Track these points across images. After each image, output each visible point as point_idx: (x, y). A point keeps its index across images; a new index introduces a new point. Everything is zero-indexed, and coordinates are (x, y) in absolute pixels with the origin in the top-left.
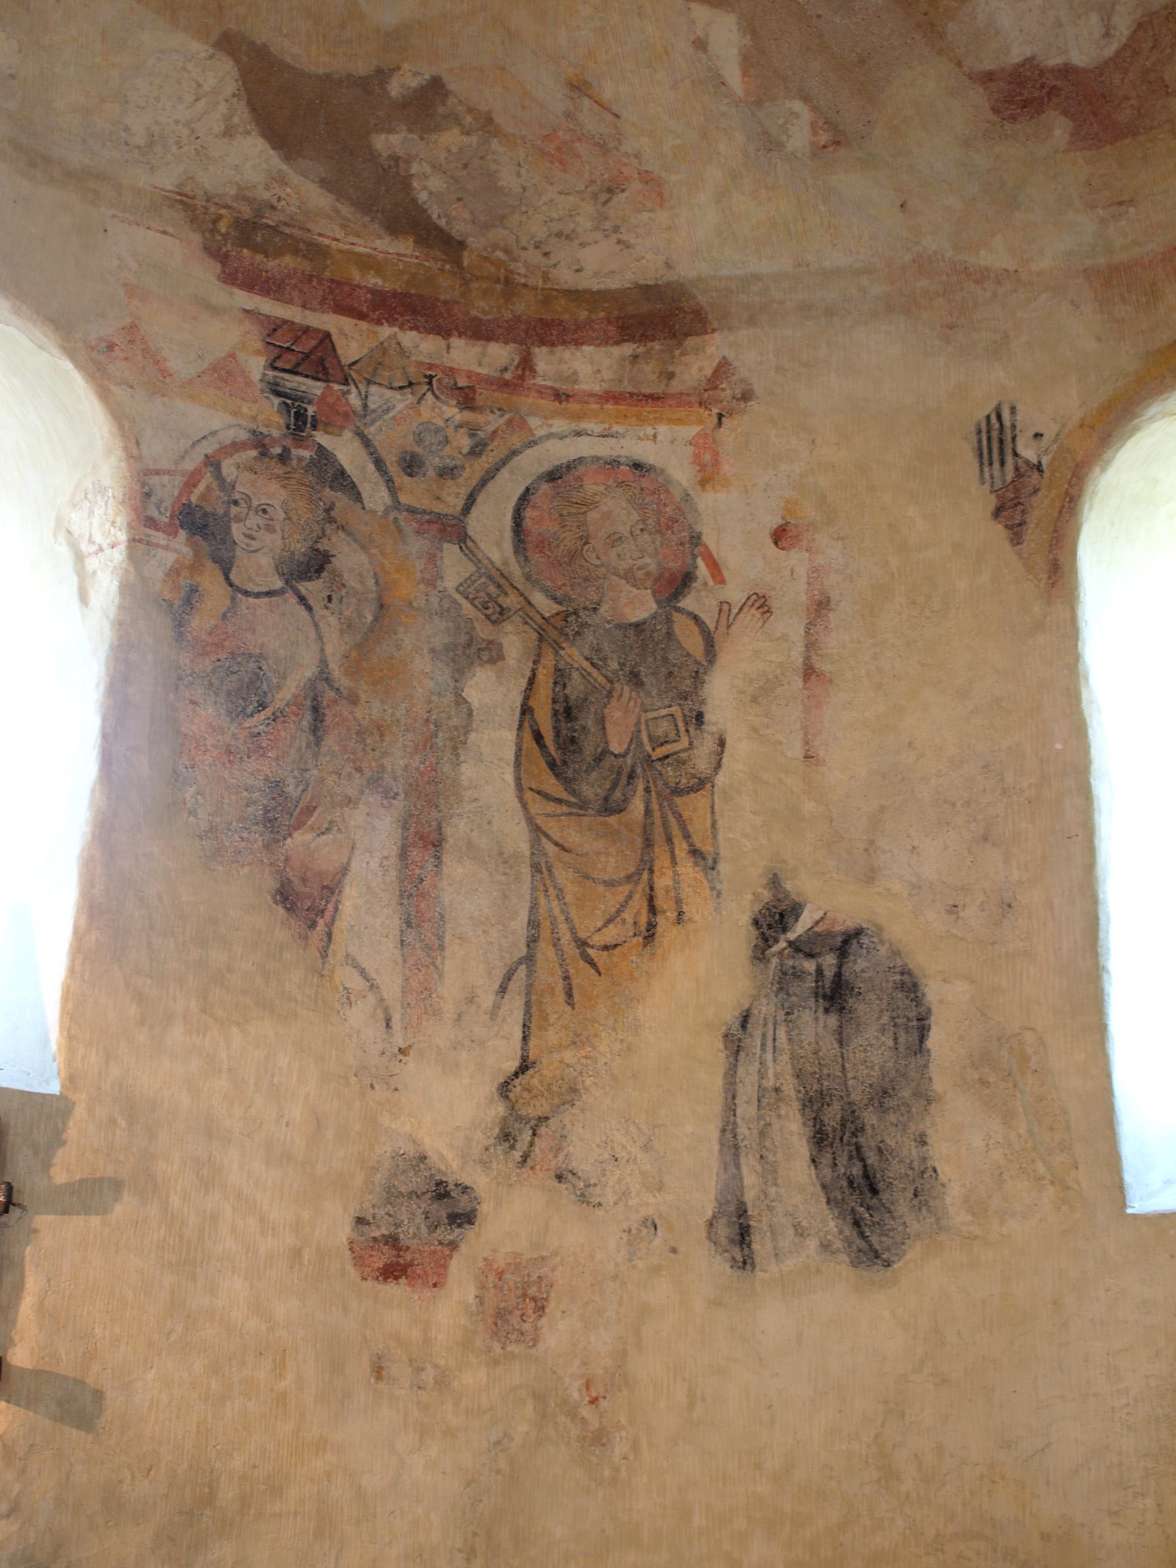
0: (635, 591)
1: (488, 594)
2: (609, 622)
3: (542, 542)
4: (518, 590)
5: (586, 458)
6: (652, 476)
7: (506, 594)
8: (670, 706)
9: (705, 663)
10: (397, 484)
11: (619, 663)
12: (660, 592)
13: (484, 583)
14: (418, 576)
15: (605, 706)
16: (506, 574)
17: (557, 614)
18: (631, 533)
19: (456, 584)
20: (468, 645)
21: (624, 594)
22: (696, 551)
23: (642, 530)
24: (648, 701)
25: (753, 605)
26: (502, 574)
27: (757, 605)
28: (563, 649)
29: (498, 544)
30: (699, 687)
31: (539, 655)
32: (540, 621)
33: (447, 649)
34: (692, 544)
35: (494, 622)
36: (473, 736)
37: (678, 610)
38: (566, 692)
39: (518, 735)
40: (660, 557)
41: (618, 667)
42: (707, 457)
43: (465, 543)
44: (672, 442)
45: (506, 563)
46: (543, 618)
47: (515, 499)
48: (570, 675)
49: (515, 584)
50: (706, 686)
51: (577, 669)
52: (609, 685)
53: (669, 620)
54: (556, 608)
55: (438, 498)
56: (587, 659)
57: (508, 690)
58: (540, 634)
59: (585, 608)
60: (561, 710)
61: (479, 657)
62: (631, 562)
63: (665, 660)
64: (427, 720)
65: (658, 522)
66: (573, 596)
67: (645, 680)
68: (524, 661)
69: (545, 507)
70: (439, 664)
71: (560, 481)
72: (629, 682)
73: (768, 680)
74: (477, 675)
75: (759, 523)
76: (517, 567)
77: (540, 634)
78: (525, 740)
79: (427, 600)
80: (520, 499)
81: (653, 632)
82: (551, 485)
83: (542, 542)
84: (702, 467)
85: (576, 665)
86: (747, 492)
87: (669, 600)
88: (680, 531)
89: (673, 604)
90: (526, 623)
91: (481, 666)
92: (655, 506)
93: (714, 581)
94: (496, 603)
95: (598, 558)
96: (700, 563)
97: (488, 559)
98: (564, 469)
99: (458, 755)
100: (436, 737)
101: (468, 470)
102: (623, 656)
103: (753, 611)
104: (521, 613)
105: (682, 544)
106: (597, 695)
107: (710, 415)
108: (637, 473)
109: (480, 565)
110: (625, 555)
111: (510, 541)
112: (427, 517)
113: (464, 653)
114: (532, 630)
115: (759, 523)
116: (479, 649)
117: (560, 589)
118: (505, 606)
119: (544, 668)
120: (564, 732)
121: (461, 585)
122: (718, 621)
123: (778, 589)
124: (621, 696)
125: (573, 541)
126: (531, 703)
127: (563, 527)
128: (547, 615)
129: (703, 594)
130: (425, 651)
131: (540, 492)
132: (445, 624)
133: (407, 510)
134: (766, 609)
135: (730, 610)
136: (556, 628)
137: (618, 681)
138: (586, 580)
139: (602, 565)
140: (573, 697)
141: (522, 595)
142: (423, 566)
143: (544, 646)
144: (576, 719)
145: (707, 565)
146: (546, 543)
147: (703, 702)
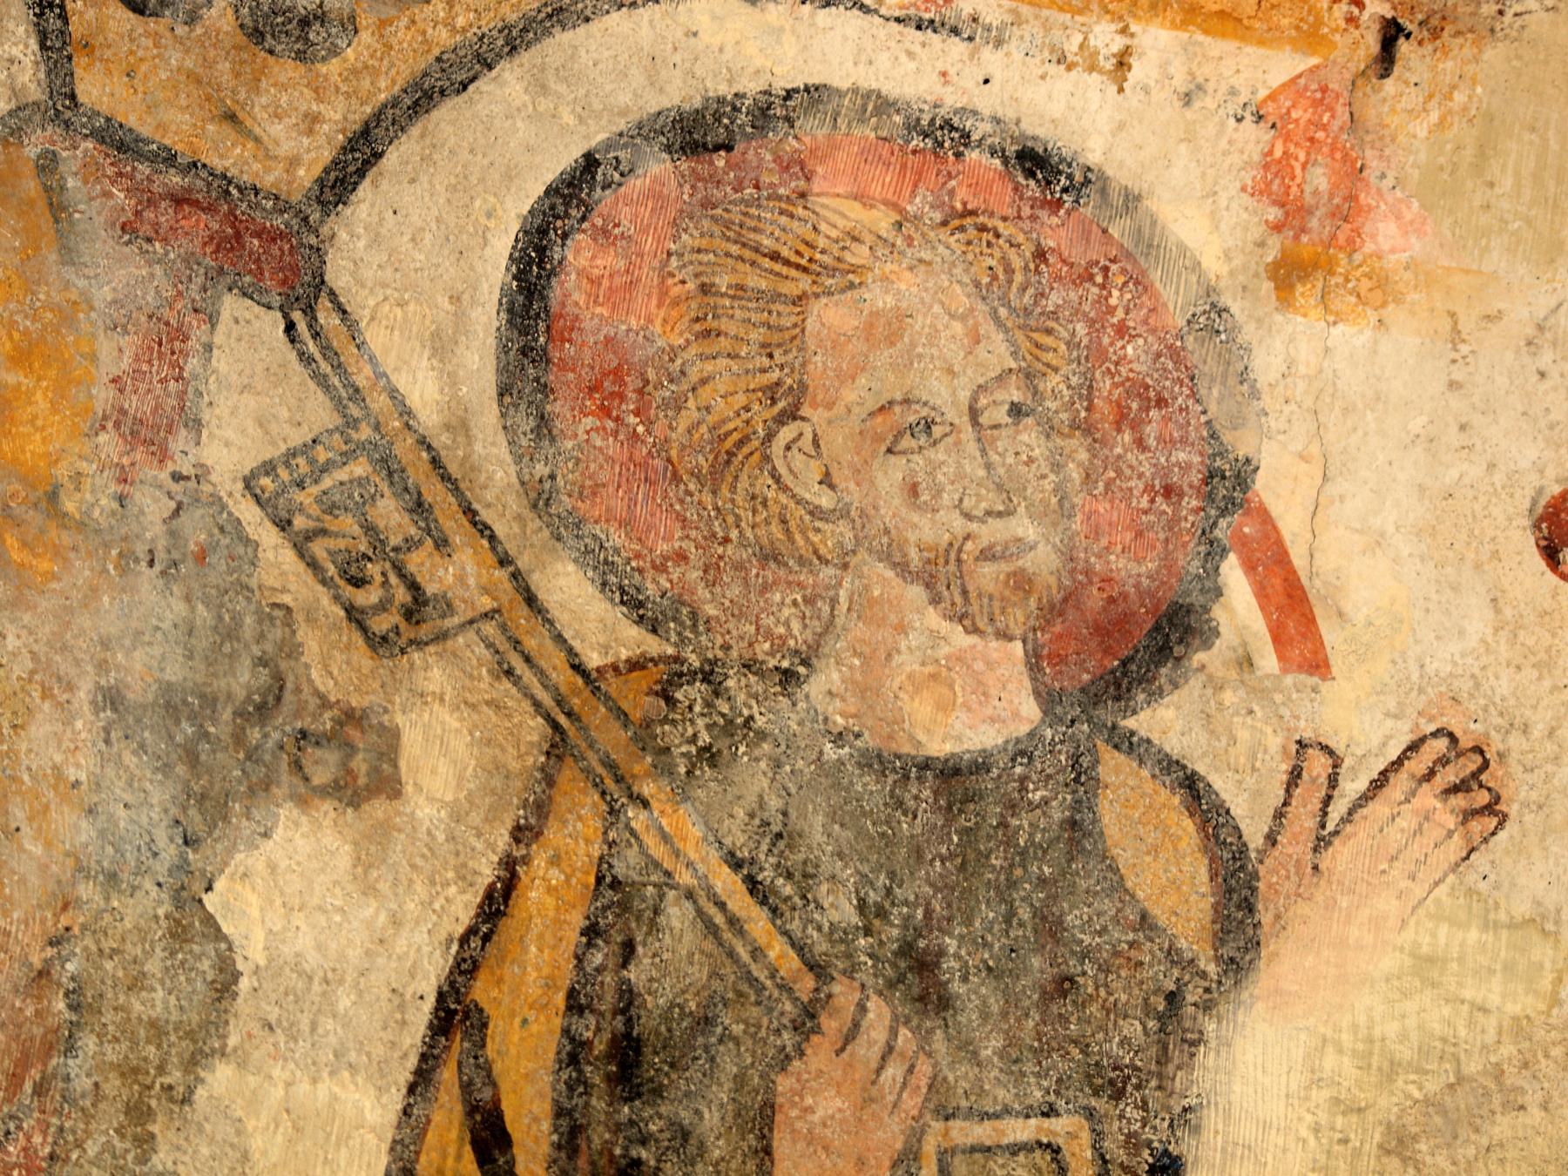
0: (960, 638)
1: (369, 529)
2: (839, 738)
3: (617, 374)
4: (492, 538)
5: (841, 94)
6: (1087, 211)
7: (442, 544)
8: (1050, 1112)
9: (1212, 969)
10: (76, 27)
11: (862, 906)
12: (1058, 659)
13: (361, 482)
14: (103, 397)
15: (783, 1061)
16: (454, 469)
17: (635, 665)
18: (974, 414)
19: (248, 466)
20: (263, 708)
21: (914, 639)
22: (1222, 532)
23: (1016, 411)
24: (960, 1076)
25: (1430, 775)
26: (436, 462)
27: (1449, 776)
28: (645, 804)
29: (441, 346)
30: (1176, 1056)
31: (541, 809)
32: (563, 676)
33: (171, 705)
34: (1210, 497)
35: (379, 643)
36: (220, 1078)
37: (1128, 744)
38: (632, 974)
39: (406, 1112)
40: (1077, 524)
41: (855, 920)
42: (1319, 179)
43: (310, 311)
44: (1187, 99)
45: (460, 426)
46: (578, 668)
47: (534, 189)
48: (657, 911)
49: (485, 515)
50: (1206, 1058)
51: (690, 895)
52: (808, 982)
53: (1082, 776)
54: (632, 640)
55: (231, 118)
56: (736, 864)
57: (396, 922)
58: (556, 726)
59: (748, 666)
60: (600, 1047)
61: (297, 766)
62: (958, 524)
63: (1050, 928)
64: (43, 974)
65: (1088, 391)
66: (711, 610)
67: (957, 987)
68: (476, 818)
69: (649, 244)
70: (130, 759)
71: (720, 160)
72: (891, 985)
73: (1461, 1079)
74: (279, 834)
75: (1491, 466)
76: (502, 450)
77: (556, 726)
78: (431, 1137)
79: (121, 499)
80: (551, 191)
81: (1012, 807)
82: (684, 165)
83: (617, 374)
84: (1293, 215)
85: (685, 878)
86: (1456, 337)
87: (1092, 697)
88: (1167, 442)
89: (1105, 714)
90: (509, 673)
91: (302, 802)
92: (1081, 329)
93: (1281, 657)
94: (402, 575)
95: (827, 481)
96: (1232, 572)
97: (393, 393)
98: (742, 118)
99: (146, 1143)
100: (70, 1049)
101: (365, 36)
102: (883, 879)
103: (1427, 797)
104: (489, 629)
105: (1168, 491)
106: (755, 1011)
107: (1351, 20)
108: (1032, 188)
109: (355, 411)
110: (938, 492)
111: (491, 342)
112: (175, 179)
113: (239, 739)
114: (527, 705)
115: (1491, 466)
116: (304, 734)
117: (661, 568)
118: (431, 589)
119: (555, 861)
120: (598, 1136)
121: (269, 468)
122: (1279, 815)
123: (1537, 731)
124: (851, 1035)
125: (741, 399)
126: (481, 991)
127: (707, 333)
128: (594, 660)
129: (1228, 697)
130: (83, 695)
131: (636, 184)
132: (180, 607)
133: (100, 136)
134: (1483, 798)
135: (1333, 782)
136: (623, 717)
137: (850, 973)
138: (769, 556)
139: (843, 513)
140: (655, 1003)
141: (504, 561)
142: (126, 362)
143: (568, 774)
144: (658, 1092)
145: (1262, 594)
146: (632, 382)
147: (1186, 1118)
